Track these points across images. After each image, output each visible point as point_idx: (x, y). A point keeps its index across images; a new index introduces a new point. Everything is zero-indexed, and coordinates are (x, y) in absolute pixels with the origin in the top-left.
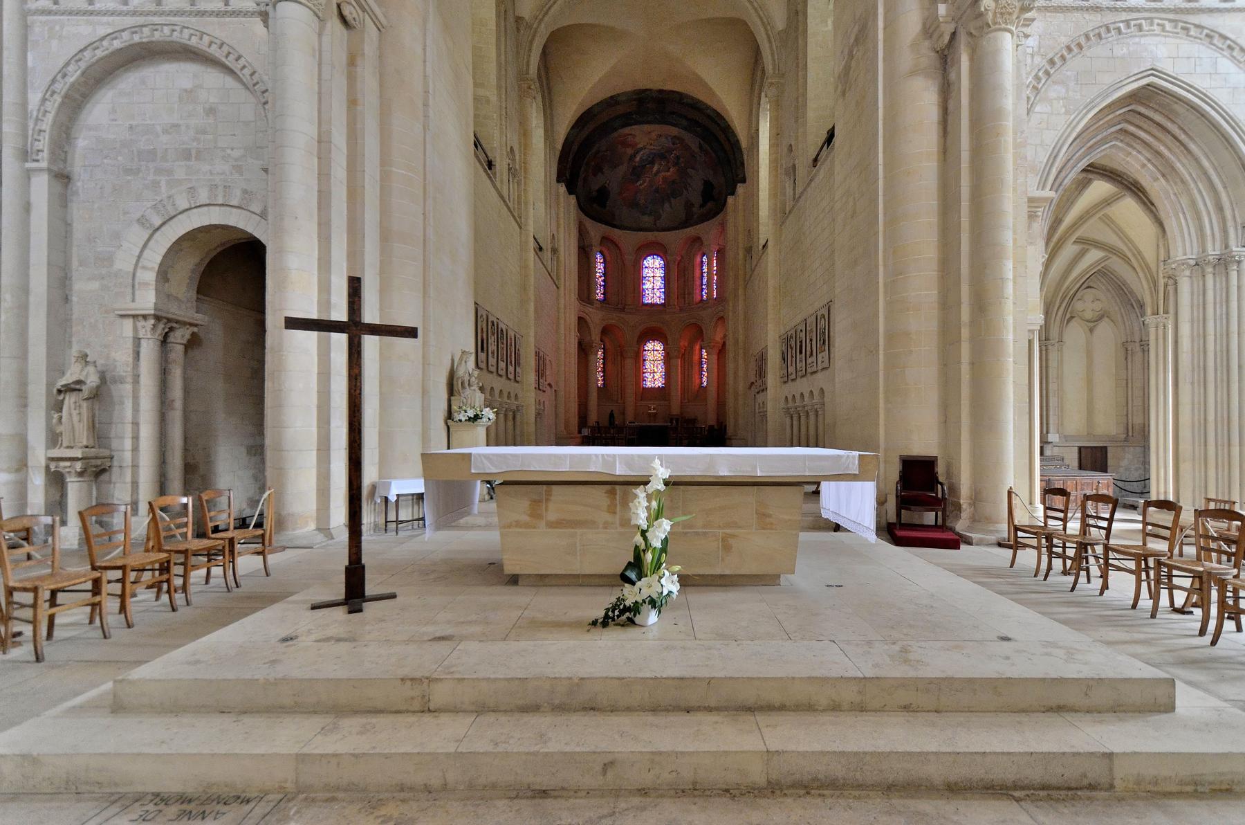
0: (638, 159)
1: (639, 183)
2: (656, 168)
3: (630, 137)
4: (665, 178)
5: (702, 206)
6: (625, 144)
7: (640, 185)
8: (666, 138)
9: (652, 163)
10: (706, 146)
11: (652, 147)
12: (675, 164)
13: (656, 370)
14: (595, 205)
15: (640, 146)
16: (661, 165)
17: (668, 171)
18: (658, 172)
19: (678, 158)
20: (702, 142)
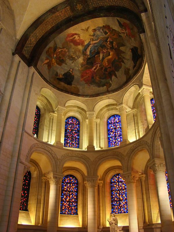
0: (88, 53)
1: (93, 69)
2: (101, 55)
3: (76, 36)
4: (109, 61)
5: (134, 68)
6: (76, 43)
7: (95, 69)
8: (99, 30)
9: (98, 53)
10: (123, 21)
11: (94, 42)
12: (112, 48)
13: (121, 199)
14: (62, 84)
15: (86, 43)
16: (104, 53)
17: (109, 55)
18: (103, 58)
19: (111, 43)
20: (118, 18)
